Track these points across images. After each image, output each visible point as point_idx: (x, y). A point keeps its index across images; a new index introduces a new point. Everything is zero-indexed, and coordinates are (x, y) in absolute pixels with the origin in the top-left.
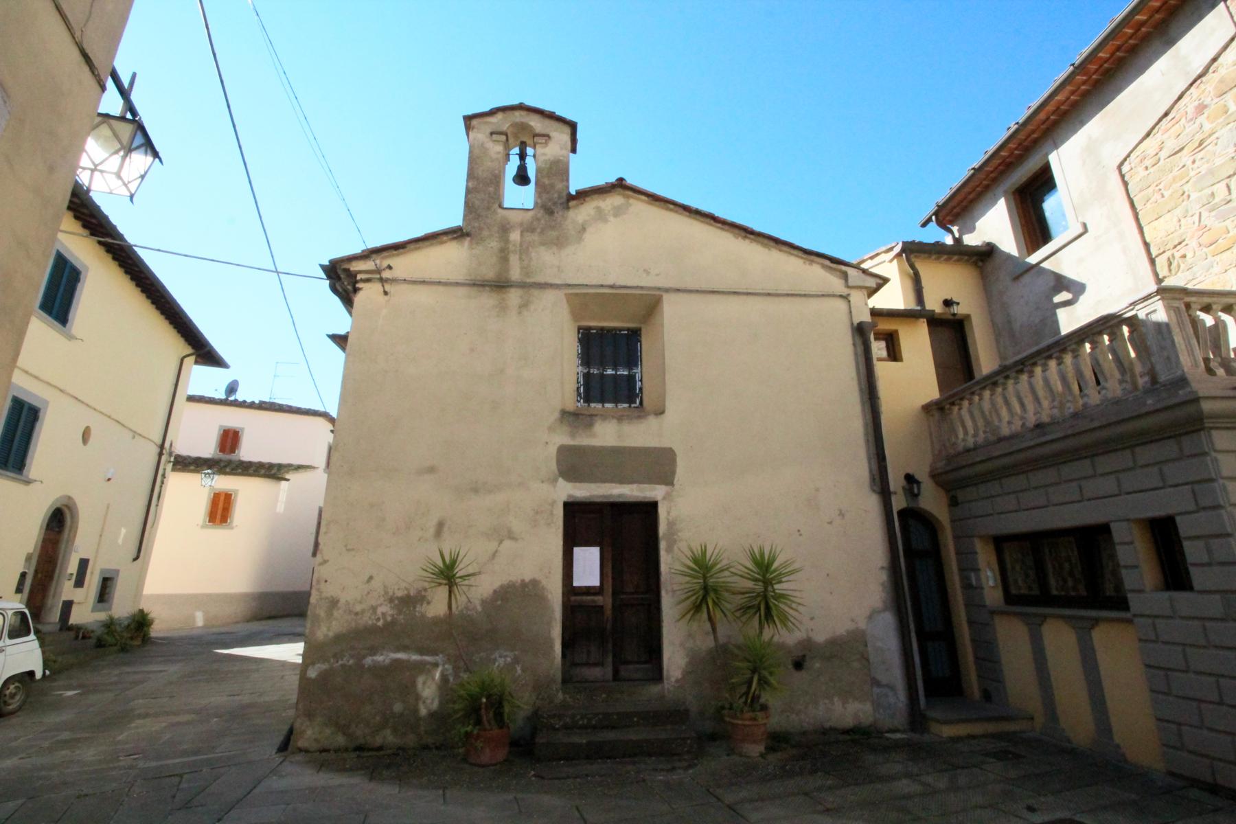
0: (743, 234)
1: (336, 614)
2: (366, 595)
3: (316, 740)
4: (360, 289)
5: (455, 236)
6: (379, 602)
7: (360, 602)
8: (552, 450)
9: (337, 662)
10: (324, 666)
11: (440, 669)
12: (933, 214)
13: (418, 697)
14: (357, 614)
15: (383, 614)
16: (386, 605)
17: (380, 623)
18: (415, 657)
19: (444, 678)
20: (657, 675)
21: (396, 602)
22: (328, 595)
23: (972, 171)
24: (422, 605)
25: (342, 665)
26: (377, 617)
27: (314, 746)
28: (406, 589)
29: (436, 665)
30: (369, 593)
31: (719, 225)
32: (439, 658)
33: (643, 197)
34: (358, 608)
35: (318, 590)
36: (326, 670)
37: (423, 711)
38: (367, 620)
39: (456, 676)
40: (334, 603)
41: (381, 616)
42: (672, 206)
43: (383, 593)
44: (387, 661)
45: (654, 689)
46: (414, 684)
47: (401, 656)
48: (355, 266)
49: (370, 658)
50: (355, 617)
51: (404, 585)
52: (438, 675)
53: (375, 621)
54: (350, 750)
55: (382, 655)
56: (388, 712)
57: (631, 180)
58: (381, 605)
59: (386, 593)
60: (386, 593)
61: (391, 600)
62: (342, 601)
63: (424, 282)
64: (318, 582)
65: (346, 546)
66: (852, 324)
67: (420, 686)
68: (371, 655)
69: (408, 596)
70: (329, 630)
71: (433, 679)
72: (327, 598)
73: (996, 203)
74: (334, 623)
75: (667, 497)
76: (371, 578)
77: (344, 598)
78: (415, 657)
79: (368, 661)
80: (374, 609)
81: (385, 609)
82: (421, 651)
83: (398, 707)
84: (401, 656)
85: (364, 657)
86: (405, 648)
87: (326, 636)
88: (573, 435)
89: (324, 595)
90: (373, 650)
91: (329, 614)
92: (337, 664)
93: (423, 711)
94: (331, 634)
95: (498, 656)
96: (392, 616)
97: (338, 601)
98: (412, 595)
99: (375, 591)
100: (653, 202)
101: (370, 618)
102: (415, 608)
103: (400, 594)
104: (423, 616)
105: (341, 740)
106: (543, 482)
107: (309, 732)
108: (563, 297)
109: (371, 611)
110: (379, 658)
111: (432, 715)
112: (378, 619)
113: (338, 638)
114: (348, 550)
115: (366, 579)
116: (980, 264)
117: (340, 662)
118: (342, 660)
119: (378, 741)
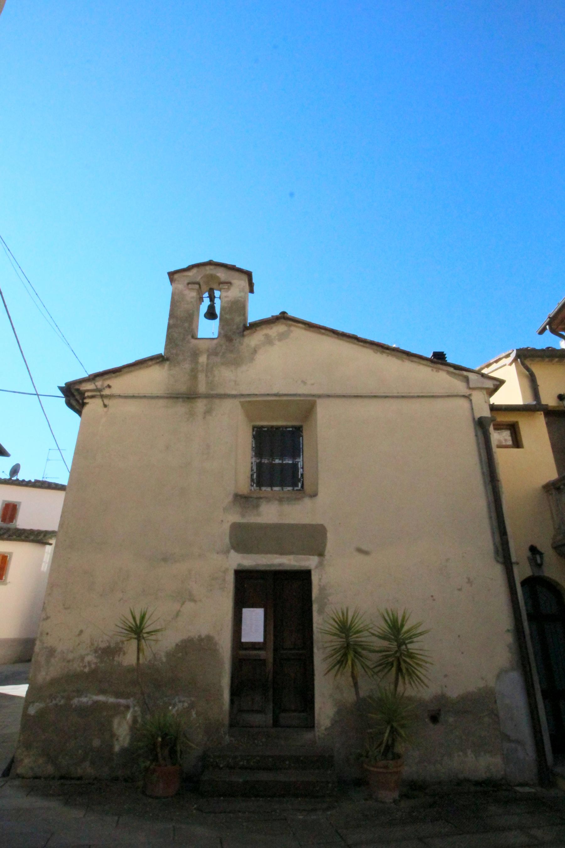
3: (32, 768)
4: (87, 403)
5: (158, 361)
7: (72, 652)
8: (226, 527)
9: (52, 701)
11: (131, 710)
12: (547, 324)
13: (113, 735)
14: (69, 661)
15: (89, 663)
18: (112, 700)
19: (135, 721)
20: (310, 725)
24: (119, 656)
25: (56, 705)
26: (84, 665)
27: (30, 774)
29: (128, 707)
30: (79, 644)
31: (362, 344)
34: (70, 656)
37: (117, 748)
38: (77, 667)
40: (51, 652)
41: (87, 664)
42: (323, 331)
44: (90, 703)
45: (308, 736)
46: (110, 723)
47: (101, 698)
48: (85, 387)
52: (129, 716)
53: (82, 668)
55: (86, 697)
57: (291, 313)
58: (88, 654)
60: (92, 644)
61: (96, 651)
62: (59, 650)
65: (64, 605)
68: (78, 697)
69: (109, 647)
70: (47, 674)
72: (47, 648)
76: (81, 632)
78: (112, 700)
79: (75, 701)
80: (82, 658)
82: (118, 695)
83: (96, 743)
84: (101, 698)
86: (103, 692)
88: (243, 516)
89: (45, 645)
90: (80, 693)
91: (48, 662)
92: (51, 704)
93: (117, 748)
94: (48, 678)
96: (96, 663)
97: (55, 651)
102: (113, 658)
103: (103, 645)
104: (120, 664)
105: (50, 769)
107: (26, 761)
110: (84, 700)
111: (124, 751)
112: (85, 667)
113: (54, 682)
114: (66, 609)
115: (77, 633)
117: (54, 702)
118: (55, 700)
119: (80, 771)
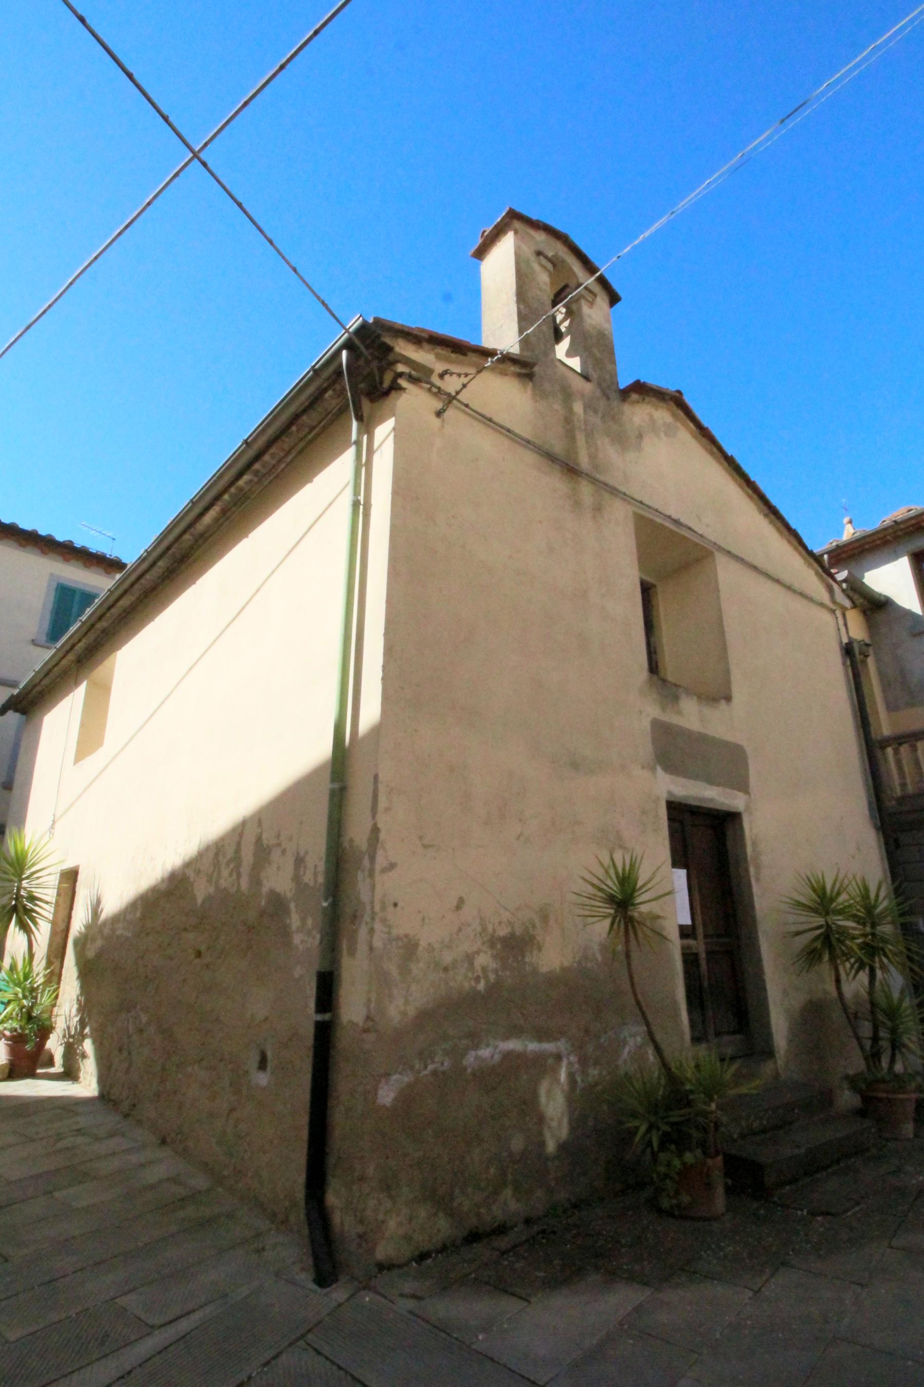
0: (767, 511)
1: (417, 968)
2: (457, 934)
3: (408, 1238)
4: (401, 389)
5: (523, 371)
6: (475, 948)
7: (449, 947)
8: (646, 724)
9: (426, 1067)
10: (407, 1079)
11: (564, 1063)
12: (826, 553)
13: (541, 1119)
14: (446, 969)
15: (484, 969)
16: (486, 952)
17: (481, 986)
18: (533, 1046)
20: (769, 1053)
21: (499, 946)
22: (401, 932)
23: (893, 523)
24: (531, 952)
25: (435, 1073)
26: (475, 975)
27: (407, 1251)
28: (510, 923)
29: (558, 1057)
30: (460, 930)
31: (750, 492)
32: (561, 1046)
33: (692, 425)
34: (448, 958)
35: (384, 921)
36: (409, 1085)
37: (551, 1146)
38: (461, 981)
39: (584, 1072)
40: (410, 948)
41: (480, 973)
42: (715, 450)
43: (479, 929)
44: (497, 1057)
45: (767, 1069)
46: (535, 1095)
47: (513, 1045)
48: (404, 348)
49: (473, 1053)
50: (444, 976)
51: (506, 916)
52: (563, 1076)
53: (473, 983)
54: (126, 1375)
55: (488, 1045)
56: (505, 1154)
57: (688, 399)
58: (478, 952)
59: (484, 929)
60: (484, 929)
61: (492, 944)
62: (423, 944)
63: (490, 420)
64: (384, 908)
65: (421, 838)
66: (841, 643)
67: (543, 1099)
68: (473, 1049)
69: (512, 935)
70: (406, 1003)
71: (558, 1081)
72: (398, 938)
73: (897, 560)
74: (414, 987)
75: (748, 807)
76: (461, 901)
77: (428, 936)
78: (533, 1046)
79: (470, 1059)
80: (470, 959)
81: (484, 960)
82: (542, 1035)
83: (517, 1143)
84: (513, 1045)
85: (463, 1055)
86: (515, 1031)
87: (404, 1014)
88: (663, 709)
89: (395, 932)
90: (475, 1039)
91: (404, 970)
92: (425, 1072)
93: (551, 1146)
94: (411, 1011)
95: (627, 1034)
96: (496, 971)
97: (416, 945)
98: (518, 933)
99: (469, 925)
100: (700, 437)
101: (466, 977)
102: (523, 956)
103: (503, 932)
104: (535, 971)
105: (443, 1228)
106: (643, 768)
107: (392, 1224)
108: (630, 514)
109: (466, 965)
110: (485, 1052)
111: (563, 1147)
112: (477, 979)
113: (424, 1017)
114: (425, 847)
115: (455, 903)
116: (869, 613)
117: (431, 1067)
118: (433, 1062)
119: (497, 1211)
